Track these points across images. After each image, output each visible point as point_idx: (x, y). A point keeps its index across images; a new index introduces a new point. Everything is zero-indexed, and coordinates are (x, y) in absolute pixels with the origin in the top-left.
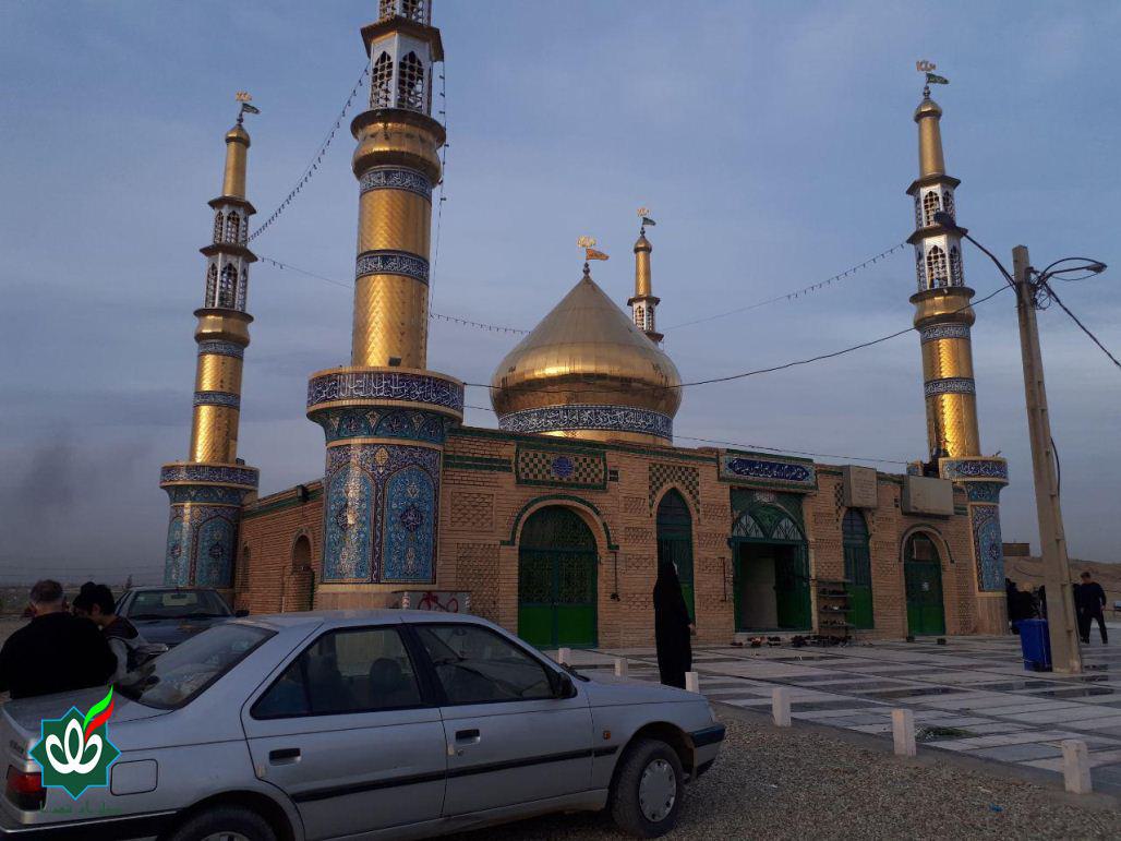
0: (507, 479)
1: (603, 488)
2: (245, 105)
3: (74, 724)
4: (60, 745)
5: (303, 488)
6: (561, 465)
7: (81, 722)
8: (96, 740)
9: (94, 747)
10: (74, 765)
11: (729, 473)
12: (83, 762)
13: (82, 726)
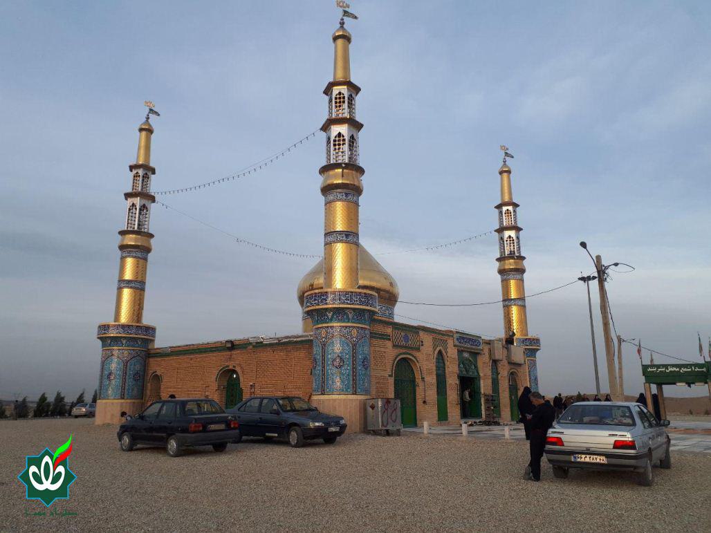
0: (389, 344)
1: (418, 349)
2: (151, 110)
3: (47, 459)
4: (38, 472)
5: (231, 342)
6: (406, 338)
7: (51, 457)
8: (61, 469)
9: (60, 473)
10: (47, 485)
11: (458, 344)
12: (53, 483)
13: (52, 460)
